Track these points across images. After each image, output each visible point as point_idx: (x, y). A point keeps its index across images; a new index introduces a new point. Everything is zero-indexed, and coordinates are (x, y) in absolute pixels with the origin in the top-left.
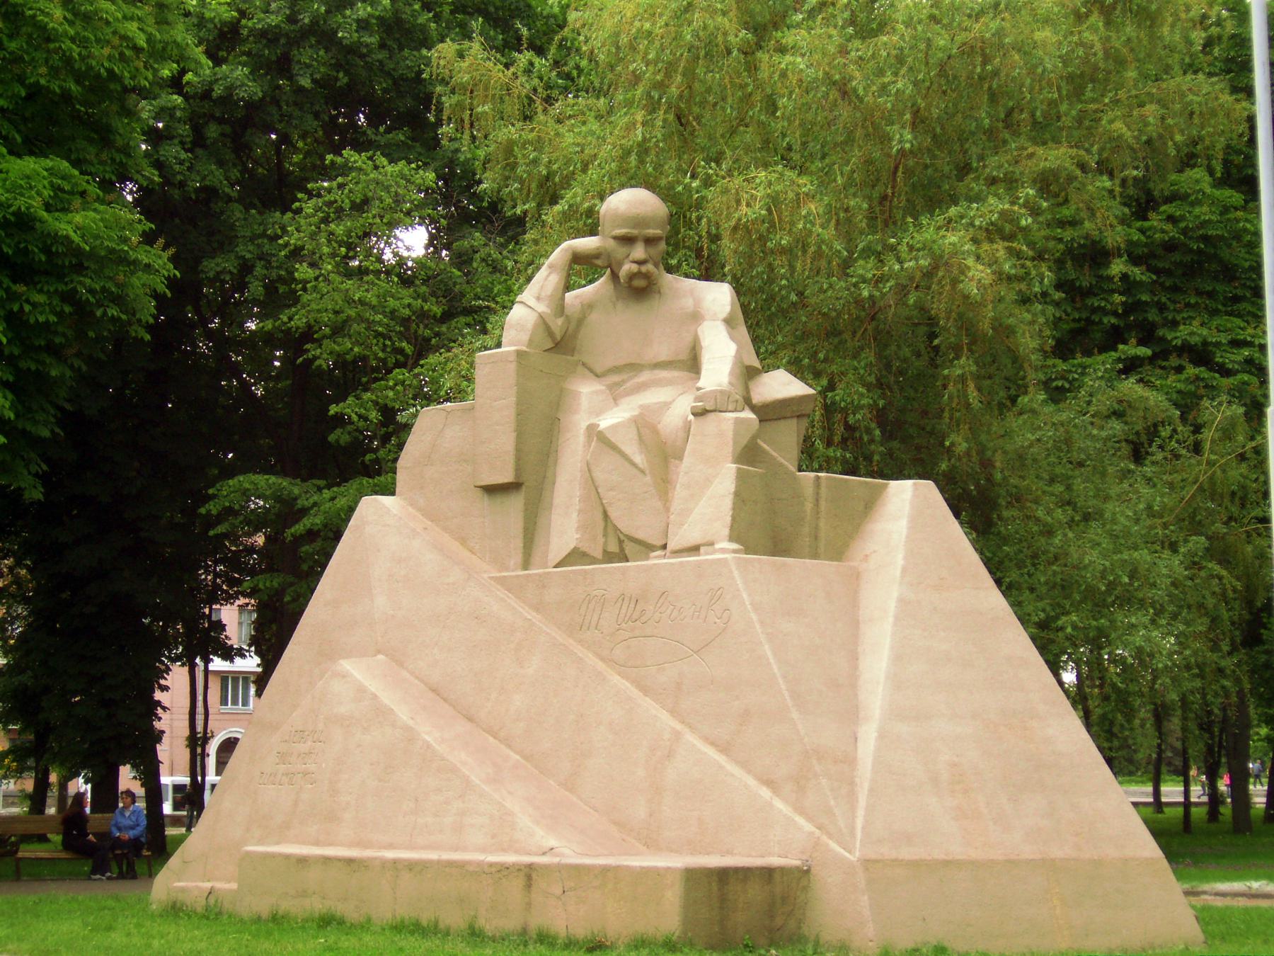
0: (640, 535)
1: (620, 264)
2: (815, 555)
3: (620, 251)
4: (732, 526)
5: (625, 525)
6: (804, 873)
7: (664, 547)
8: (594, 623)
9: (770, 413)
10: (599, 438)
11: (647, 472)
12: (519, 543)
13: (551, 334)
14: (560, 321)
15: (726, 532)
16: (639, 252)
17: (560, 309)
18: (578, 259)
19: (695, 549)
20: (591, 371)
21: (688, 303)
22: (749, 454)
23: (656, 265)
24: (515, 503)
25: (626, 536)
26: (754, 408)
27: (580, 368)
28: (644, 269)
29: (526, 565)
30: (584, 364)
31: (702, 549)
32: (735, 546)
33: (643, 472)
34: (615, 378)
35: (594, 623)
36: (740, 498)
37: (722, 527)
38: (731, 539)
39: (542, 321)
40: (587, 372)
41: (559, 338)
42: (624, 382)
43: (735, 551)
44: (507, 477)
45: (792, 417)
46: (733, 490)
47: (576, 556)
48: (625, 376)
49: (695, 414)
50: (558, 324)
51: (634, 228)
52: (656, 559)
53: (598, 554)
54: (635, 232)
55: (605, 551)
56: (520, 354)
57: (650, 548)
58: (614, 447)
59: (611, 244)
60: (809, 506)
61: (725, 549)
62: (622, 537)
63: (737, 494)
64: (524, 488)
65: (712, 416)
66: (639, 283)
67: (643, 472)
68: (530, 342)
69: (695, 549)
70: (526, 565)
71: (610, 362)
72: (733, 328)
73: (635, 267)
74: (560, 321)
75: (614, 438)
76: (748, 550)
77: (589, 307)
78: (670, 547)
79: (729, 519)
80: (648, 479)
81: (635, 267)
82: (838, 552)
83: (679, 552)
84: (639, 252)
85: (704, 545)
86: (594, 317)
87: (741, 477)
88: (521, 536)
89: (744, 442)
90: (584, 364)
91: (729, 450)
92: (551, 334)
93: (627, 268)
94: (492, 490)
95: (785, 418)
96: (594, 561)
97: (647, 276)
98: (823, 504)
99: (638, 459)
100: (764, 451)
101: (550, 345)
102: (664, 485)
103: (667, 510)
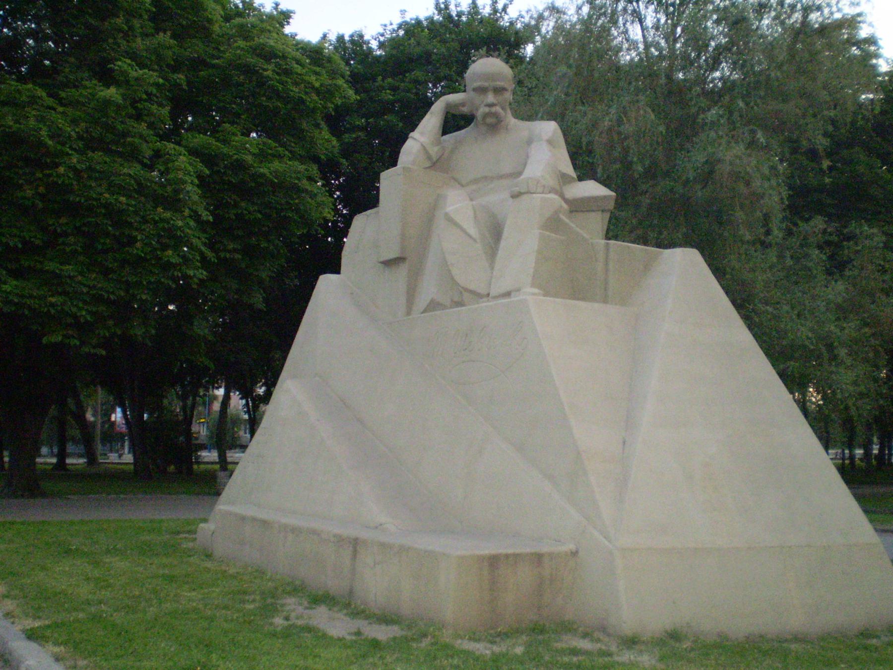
0: (472, 287)
2: (605, 301)
5: (461, 280)
7: (488, 295)
9: (578, 207)
11: (478, 241)
12: (403, 300)
13: (429, 158)
14: (436, 149)
16: (490, 98)
19: (508, 294)
20: (460, 183)
22: (553, 224)
23: (503, 108)
24: (402, 273)
25: (463, 288)
26: (566, 201)
28: (493, 109)
31: (513, 294)
32: (536, 291)
33: (475, 240)
34: (474, 187)
38: (533, 285)
41: (435, 159)
43: (534, 294)
44: (397, 255)
45: (598, 211)
46: (536, 248)
47: (433, 306)
52: (484, 304)
54: (486, 84)
55: (452, 301)
60: (600, 266)
61: (530, 295)
62: (462, 290)
64: (407, 260)
65: (525, 197)
66: (490, 120)
67: (475, 240)
69: (508, 294)
70: (409, 313)
72: (554, 147)
73: (487, 110)
74: (436, 149)
75: (458, 219)
76: (546, 294)
81: (487, 110)
84: (490, 98)
92: (429, 158)
94: (388, 263)
95: (593, 211)
97: (495, 115)
98: (611, 266)
99: (473, 231)
101: (428, 164)
102: (492, 251)
103: (492, 268)
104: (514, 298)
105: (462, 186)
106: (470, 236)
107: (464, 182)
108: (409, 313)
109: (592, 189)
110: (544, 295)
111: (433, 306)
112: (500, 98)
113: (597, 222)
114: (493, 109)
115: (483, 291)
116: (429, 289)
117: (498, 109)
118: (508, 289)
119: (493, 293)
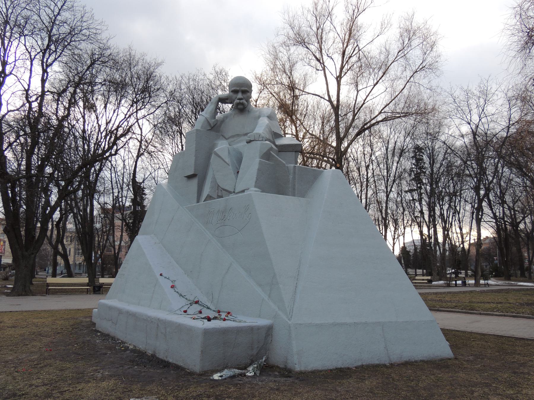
0: (226, 188)
1: (234, 101)
2: (294, 195)
3: (234, 96)
4: (256, 182)
6: (269, 330)
7: (234, 192)
8: (210, 221)
11: (230, 165)
12: (196, 195)
13: (210, 124)
14: (213, 120)
15: (254, 184)
19: (243, 191)
22: (267, 156)
24: (195, 182)
25: (222, 188)
26: (276, 146)
27: (221, 137)
28: (241, 101)
30: (222, 136)
34: (232, 139)
35: (210, 221)
36: (260, 170)
37: (253, 182)
38: (255, 187)
40: (224, 138)
41: (212, 125)
42: (235, 140)
47: (209, 197)
48: (235, 139)
49: (247, 143)
50: (212, 121)
51: (237, 87)
52: (232, 196)
53: (215, 196)
54: (238, 89)
57: (230, 192)
58: (219, 157)
61: (253, 191)
63: (259, 170)
64: (198, 176)
66: (240, 107)
68: (202, 127)
69: (243, 191)
71: (230, 134)
72: (271, 120)
73: (238, 101)
78: (236, 191)
79: (255, 179)
80: (230, 167)
81: (238, 101)
85: (246, 190)
87: (260, 163)
88: (196, 193)
89: (265, 151)
90: (222, 136)
92: (210, 124)
93: (237, 101)
96: (214, 199)
97: (242, 104)
99: (227, 160)
100: (273, 156)
103: (237, 179)
104: (246, 193)
105: (227, 139)
106: (225, 162)
107: (227, 137)
108: (198, 201)
110: (262, 192)
111: (209, 197)
114: (241, 101)
115: (232, 191)
116: (207, 191)
118: (243, 189)
119: (236, 191)
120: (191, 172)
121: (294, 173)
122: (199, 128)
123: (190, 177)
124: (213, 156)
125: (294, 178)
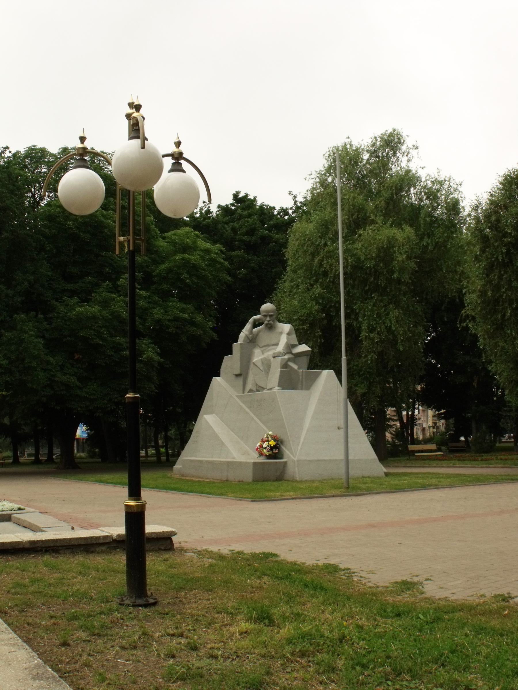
2: (302, 389)
10: (254, 363)
12: (242, 387)
15: (277, 385)
16: (268, 319)
17: (251, 332)
18: (255, 321)
19: (271, 389)
21: (280, 330)
22: (285, 366)
24: (241, 380)
29: (243, 392)
34: (264, 348)
37: (276, 383)
38: (278, 386)
39: (247, 336)
41: (250, 339)
47: (251, 391)
52: (265, 391)
53: (255, 390)
56: (241, 344)
58: (256, 366)
59: (262, 317)
63: (280, 376)
66: (269, 326)
68: (244, 341)
69: (271, 389)
70: (243, 392)
71: (263, 344)
77: (259, 332)
80: (263, 373)
82: (308, 388)
83: (269, 390)
86: (260, 334)
89: (283, 363)
91: (279, 366)
96: (254, 392)
97: (270, 324)
99: (261, 368)
101: (248, 341)
104: (273, 390)
109: (304, 348)
112: (272, 318)
113: (305, 361)
115: (265, 387)
116: (250, 385)
117: (271, 322)
119: (268, 388)
120: (238, 372)
121: (302, 375)
122: (242, 342)
123: (238, 376)
124: (252, 365)
125: (302, 378)
